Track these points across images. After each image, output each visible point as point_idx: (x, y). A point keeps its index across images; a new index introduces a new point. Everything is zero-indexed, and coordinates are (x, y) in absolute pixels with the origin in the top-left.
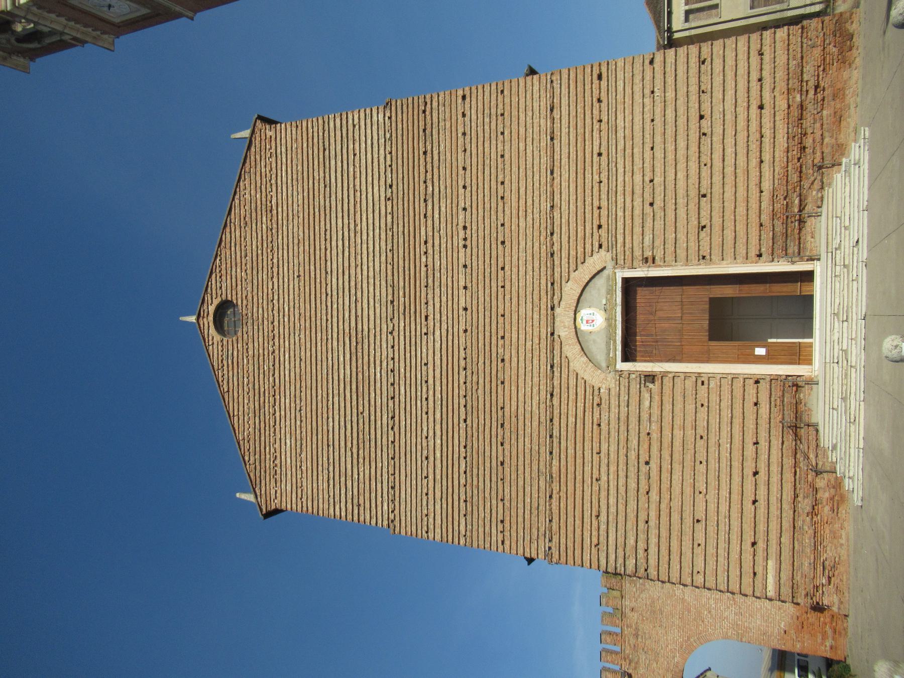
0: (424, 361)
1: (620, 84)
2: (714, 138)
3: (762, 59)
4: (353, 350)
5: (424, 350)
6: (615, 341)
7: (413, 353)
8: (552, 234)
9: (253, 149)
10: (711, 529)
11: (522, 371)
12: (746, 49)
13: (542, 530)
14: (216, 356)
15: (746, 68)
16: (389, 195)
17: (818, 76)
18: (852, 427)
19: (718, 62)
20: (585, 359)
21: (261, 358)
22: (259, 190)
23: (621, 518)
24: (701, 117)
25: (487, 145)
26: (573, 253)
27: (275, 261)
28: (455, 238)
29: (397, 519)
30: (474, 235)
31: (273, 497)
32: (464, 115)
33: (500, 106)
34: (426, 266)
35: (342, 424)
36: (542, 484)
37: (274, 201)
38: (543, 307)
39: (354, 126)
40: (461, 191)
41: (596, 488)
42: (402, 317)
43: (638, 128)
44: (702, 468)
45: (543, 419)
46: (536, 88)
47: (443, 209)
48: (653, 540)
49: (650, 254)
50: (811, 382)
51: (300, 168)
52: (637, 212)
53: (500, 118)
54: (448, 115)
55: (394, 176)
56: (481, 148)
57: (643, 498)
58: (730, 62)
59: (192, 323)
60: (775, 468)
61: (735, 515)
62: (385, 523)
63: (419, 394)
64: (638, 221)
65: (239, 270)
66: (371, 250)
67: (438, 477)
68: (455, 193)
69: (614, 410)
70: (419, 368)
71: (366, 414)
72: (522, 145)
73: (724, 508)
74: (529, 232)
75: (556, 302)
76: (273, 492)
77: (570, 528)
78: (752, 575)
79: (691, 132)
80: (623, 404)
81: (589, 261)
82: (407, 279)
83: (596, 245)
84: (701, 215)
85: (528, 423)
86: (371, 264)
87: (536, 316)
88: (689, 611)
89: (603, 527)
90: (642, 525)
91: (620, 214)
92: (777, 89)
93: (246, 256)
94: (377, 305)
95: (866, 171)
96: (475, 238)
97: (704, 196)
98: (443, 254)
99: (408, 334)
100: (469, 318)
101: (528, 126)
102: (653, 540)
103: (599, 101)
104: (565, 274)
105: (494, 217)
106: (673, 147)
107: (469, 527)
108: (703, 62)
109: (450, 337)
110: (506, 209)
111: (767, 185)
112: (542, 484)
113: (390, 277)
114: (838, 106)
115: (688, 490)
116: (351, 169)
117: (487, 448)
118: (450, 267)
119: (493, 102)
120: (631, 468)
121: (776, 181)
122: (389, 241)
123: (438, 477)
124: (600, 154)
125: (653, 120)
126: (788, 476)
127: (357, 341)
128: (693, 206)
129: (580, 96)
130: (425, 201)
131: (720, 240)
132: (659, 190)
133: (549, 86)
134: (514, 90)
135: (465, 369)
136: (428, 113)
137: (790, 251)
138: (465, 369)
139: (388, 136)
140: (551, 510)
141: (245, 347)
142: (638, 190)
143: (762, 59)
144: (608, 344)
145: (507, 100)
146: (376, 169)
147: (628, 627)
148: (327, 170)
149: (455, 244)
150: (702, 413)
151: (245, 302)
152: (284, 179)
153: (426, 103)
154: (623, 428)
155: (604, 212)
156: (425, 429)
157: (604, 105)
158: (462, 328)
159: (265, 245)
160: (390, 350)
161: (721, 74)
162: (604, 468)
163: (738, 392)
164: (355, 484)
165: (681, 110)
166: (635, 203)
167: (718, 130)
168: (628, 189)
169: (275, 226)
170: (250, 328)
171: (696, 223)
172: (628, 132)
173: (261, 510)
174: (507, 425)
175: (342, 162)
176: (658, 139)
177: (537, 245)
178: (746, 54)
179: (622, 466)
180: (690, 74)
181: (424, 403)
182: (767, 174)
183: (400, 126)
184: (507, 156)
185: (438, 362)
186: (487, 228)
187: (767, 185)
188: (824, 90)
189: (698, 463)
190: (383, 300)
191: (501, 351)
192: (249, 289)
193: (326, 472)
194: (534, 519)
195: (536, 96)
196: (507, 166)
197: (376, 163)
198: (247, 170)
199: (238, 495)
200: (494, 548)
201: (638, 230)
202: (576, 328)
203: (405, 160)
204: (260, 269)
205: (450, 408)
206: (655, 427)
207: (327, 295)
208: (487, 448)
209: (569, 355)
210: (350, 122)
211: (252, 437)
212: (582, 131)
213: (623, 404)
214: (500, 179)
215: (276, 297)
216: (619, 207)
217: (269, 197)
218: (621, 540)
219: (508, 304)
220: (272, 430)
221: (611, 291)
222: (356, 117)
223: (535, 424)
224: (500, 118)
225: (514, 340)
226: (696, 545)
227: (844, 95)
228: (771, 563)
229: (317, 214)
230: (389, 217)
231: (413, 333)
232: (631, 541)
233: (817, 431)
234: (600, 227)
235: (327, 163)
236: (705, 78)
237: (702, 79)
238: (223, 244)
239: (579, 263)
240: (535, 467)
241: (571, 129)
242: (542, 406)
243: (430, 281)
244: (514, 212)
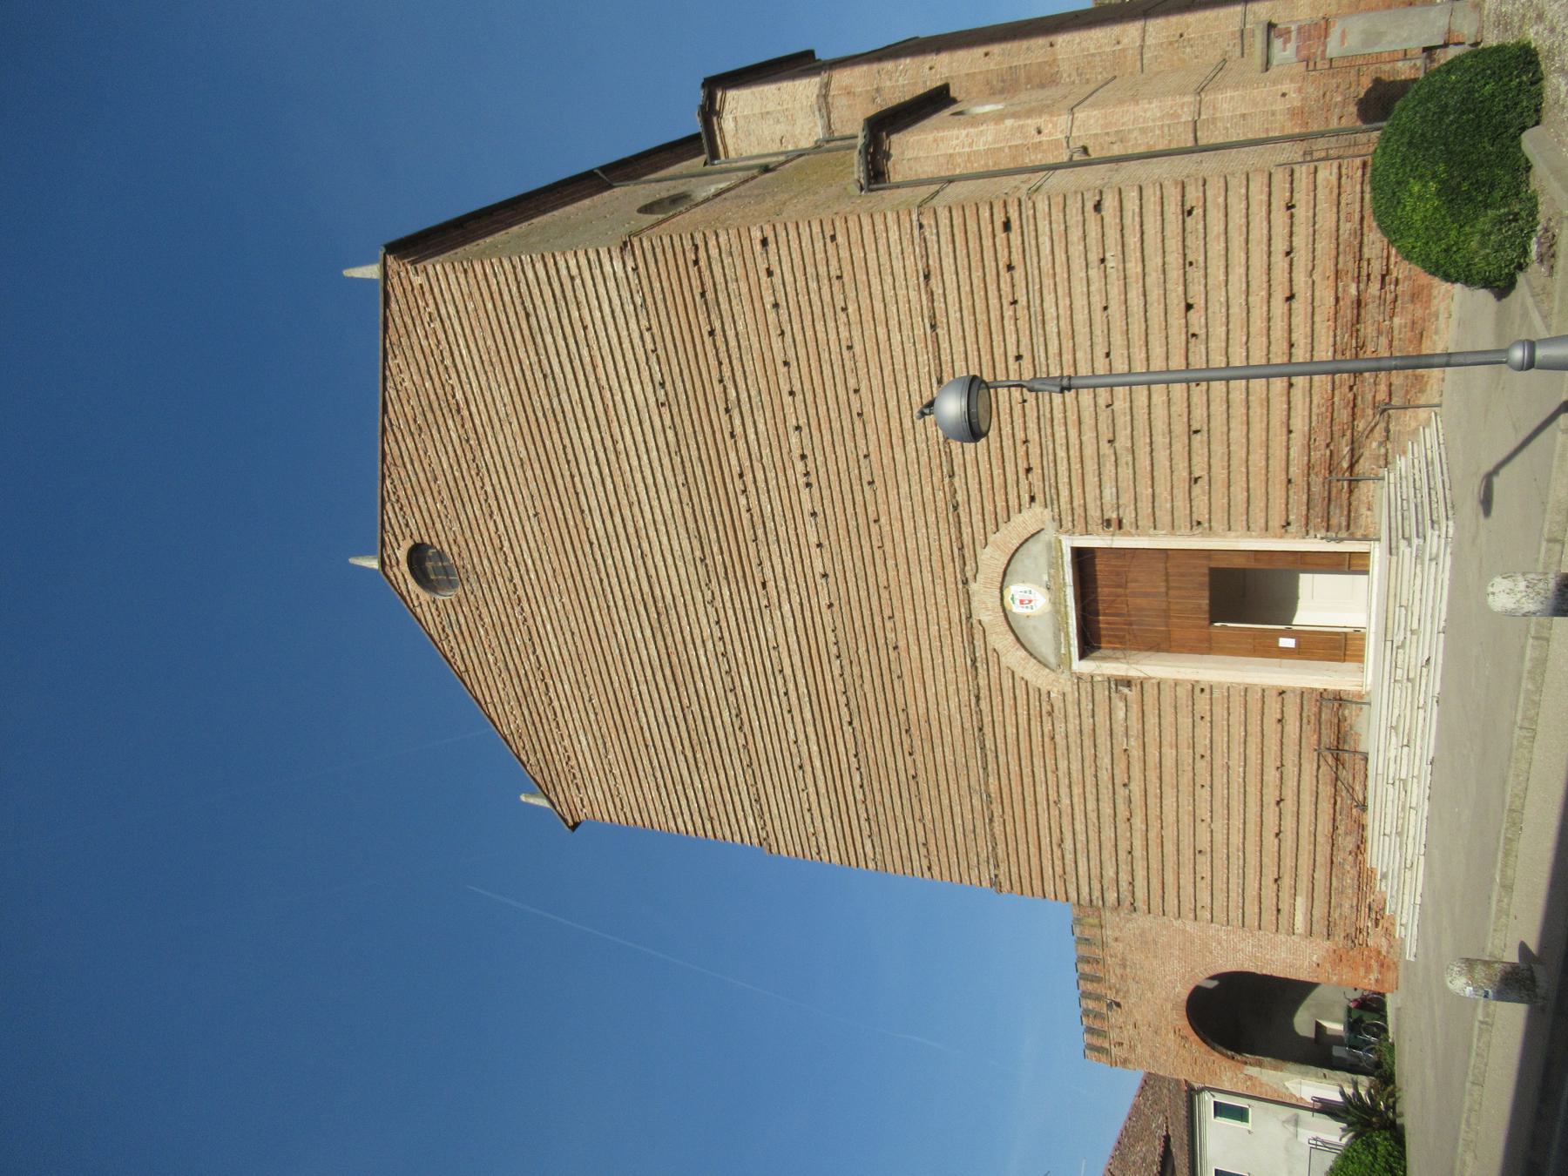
0: (772, 644)
1: (1045, 241)
2: (1212, 345)
3: (1292, 216)
4: (656, 625)
5: (769, 629)
6: (1067, 635)
7: (753, 633)
8: (952, 476)
9: (393, 305)
10: (1220, 863)
11: (927, 664)
12: (1264, 197)
13: (983, 855)
14: (429, 617)
15: (1265, 232)
16: (662, 398)
17: (1388, 258)
18: (1408, 874)
19: (1215, 216)
20: (1023, 653)
21: (507, 628)
22: (426, 377)
23: (1094, 846)
24: (1189, 307)
25: (819, 326)
26: (989, 507)
27: (489, 489)
28: (790, 472)
29: (772, 837)
30: (822, 471)
31: (579, 806)
32: (770, 273)
33: (834, 263)
34: (749, 510)
35: (661, 720)
36: (976, 802)
37: (459, 396)
38: (950, 579)
39: (572, 279)
40: (788, 399)
41: (1054, 812)
42: (724, 583)
43: (1081, 317)
44: (1206, 793)
45: (967, 725)
46: (894, 236)
47: (761, 427)
49: (1114, 516)
50: (1360, 701)
51: (490, 342)
52: (1089, 451)
53: (836, 283)
54: (740, 271)
55: (665, 369)
56: (809, 333)
57: (1122, 826)
58: (1237, 218)
59: (372, 570)
60: (1307, 798)
61: (1252, 847)
62: (755, 841)
63: (773, 687)
64: (1091, 466)
65: (430, 500)
66: (650, 481)
67: (822, 790)
68: (777, 401)
70: (766, 654)
71: (695, 707)
72: (881, 331)
73: (1236, 839)
74: (913, 469)
75: (969, 574)
76: (577, 800)
77: (1023, 857)
79: (1173, 332)
80: (1086, 714)
81: (1017, 519)
82: (721, 528)
83: (1026, 498)
84: (1194, 462)
85: (946, 730)
86: (655, 503)
87: (940, 592)
88: (1192, 943)
89: (1069, 857)
90: (1123, 855)
91: (1061, 454)
92: (1318, 270)
93: (436, 479)
94: (680, 564)
95: (1447, 582)
96: (822, 471)
97: (1196, 432)
98: (775, 494)
99: (738, 606)
100: (833, 589)
101: (888, 299)
103: (1010, 268)
104: (979, 537)
105: (850, 445)
106: (1143, 355)
107: (878, 850)
108: (1190, 213)
109: (807, 614)
110: (869, 432)
111: (1299, 424)
112: (976, 802)
113: (691, 525)
114: (1419, 313)
115: (1186, 819)
116: (585, 352)
117: (890, 759)
118: (789, 515)
119: (820, 256)
120: (1103, 790)
121: (1314, 418)
122: (679, 470)
123: (822, 790)
124: (1019, 358)
125: (1106, 308)
126: (1325, 806)
127: (660, 616)
128: (1179, 447)
129: (975, 258)
130: (727, 410)
131: (1225, 500)
132: (1123, 421)
133: (916, 232)
134: (855, 236)
135: (838, 657)
136: (703, 263)
137: (1334, 521)
138: (838, 657)
139: (639, 301)
140: (993, 835)
141: (476, 613)
143: (1292, 216)
144: (1056, 637)
145: (844, 254)
146: (629, 356)
148: (542, 351)
149: (792, 482)
150: (1203, 729)
151: (455, 549)
152: (467, 360)
153: (696, 248)
154: (1088, 743)
155: (1034, 450)
156: (791, 732)
157: (1019, 273)
158: (824, 602)
159: (464, 466)
160: (715, 629)
161: (1222, 238)
162: (1064, 791)
163: (1254, 707)
164: (700, 795)
165: (1155, 294)
166: (1084, 438)
167: (1218, 331)
168: (1072, 417)
169: (472, 435)
170: (476, 586)
171: (1185, 474)
172: (1065, 324)
173: (565, 821)
174: (914, 730)
175: (565, 338)
176: (1118, 339)
177: (928, 490)
178: (1264, 208)
179: (1090, 788)
180: (1168, 233)
181: (784, 699)
182: (1300, 406)
183: (656, 285)
184: (858, 348)
185: (794, 647)
186: (841, 460)
187: (1299, 424)
188: (1397, 282)
189: (1198, 787)
190: (689, 557)
191: (890, 635)
192: (456, 528)
193: (651, 778)
194: (971, 844)
195: (896, 250)
196: (861, 364)
197: (626, 345)
198: (394, 338)
199: (523, 798)
200: (917, 873)
201: (1092, 479)
202: (1004, 610)
203: (679, 343)
204: (466, 499)
205: (824, 706)
207: (591, 544)
208: (890, 759)
209: (998, 647)
210: (564, 272)
211: (524, 731)
212: (985, 318)
213: (1086, 714)
214: (852, 383)
215: (506, 544)
216: (1058, 442)
217: (448, 388)
218: (1095, 872)
219: (892, 573)
220: (553, 725)
221: (1055, 564)
222: (572, 263)
223: (957, 731)
224: (836, 283)
225: (910, 622)
227: (1429, 295)
228: (1301, 901)
229: (542, 420)
230: (670, 434)
231: (747, 606)
232: (1110, 872)
233: (1366, 759)
234: (1029, 470)
235: (539, 340)
236: (1195, 243)
237: (1188, 243)
238: (389, 458)
240: (964, 784)
241: (965, 313)
242: (965, 710)
243: (760, 532)
244: (883, 437)
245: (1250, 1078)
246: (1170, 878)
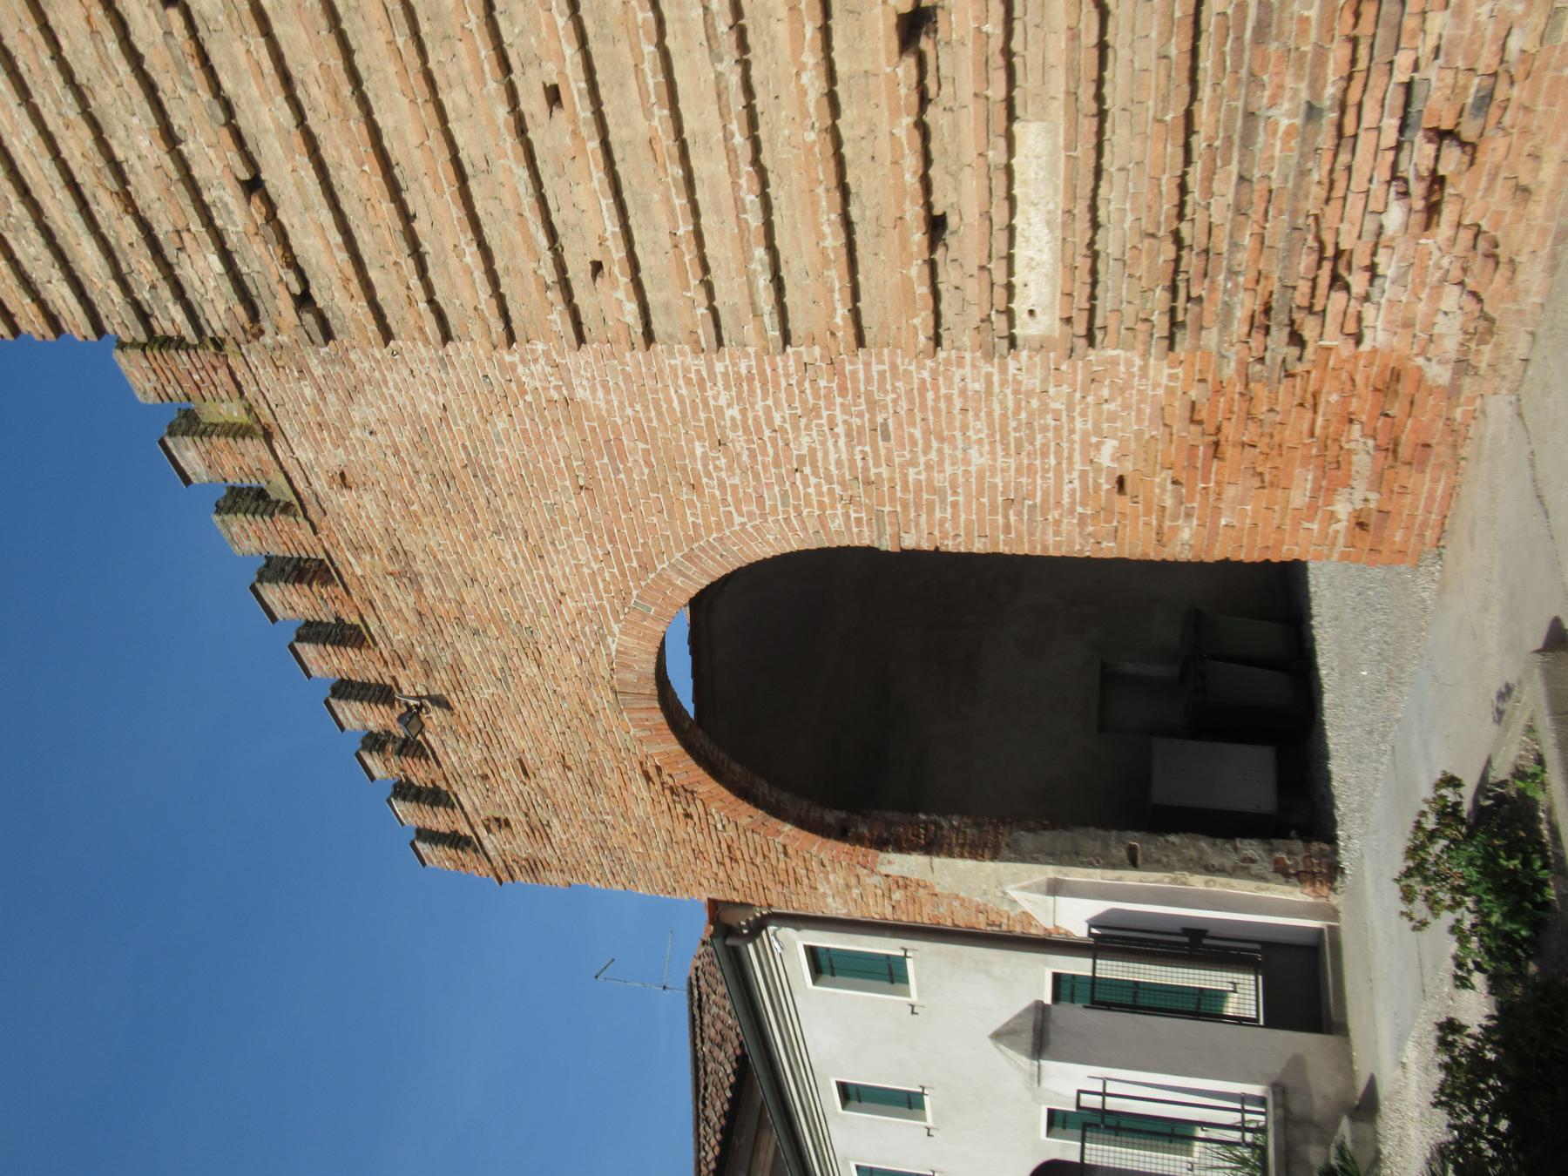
48: (265, 117)
78: (918, 238)
88: (618, 455)
102: (265, 117)
147: (356, 549)
226: (532, 103)
228: (1040, 146)
245: (903, 883)
246: (401, 117)
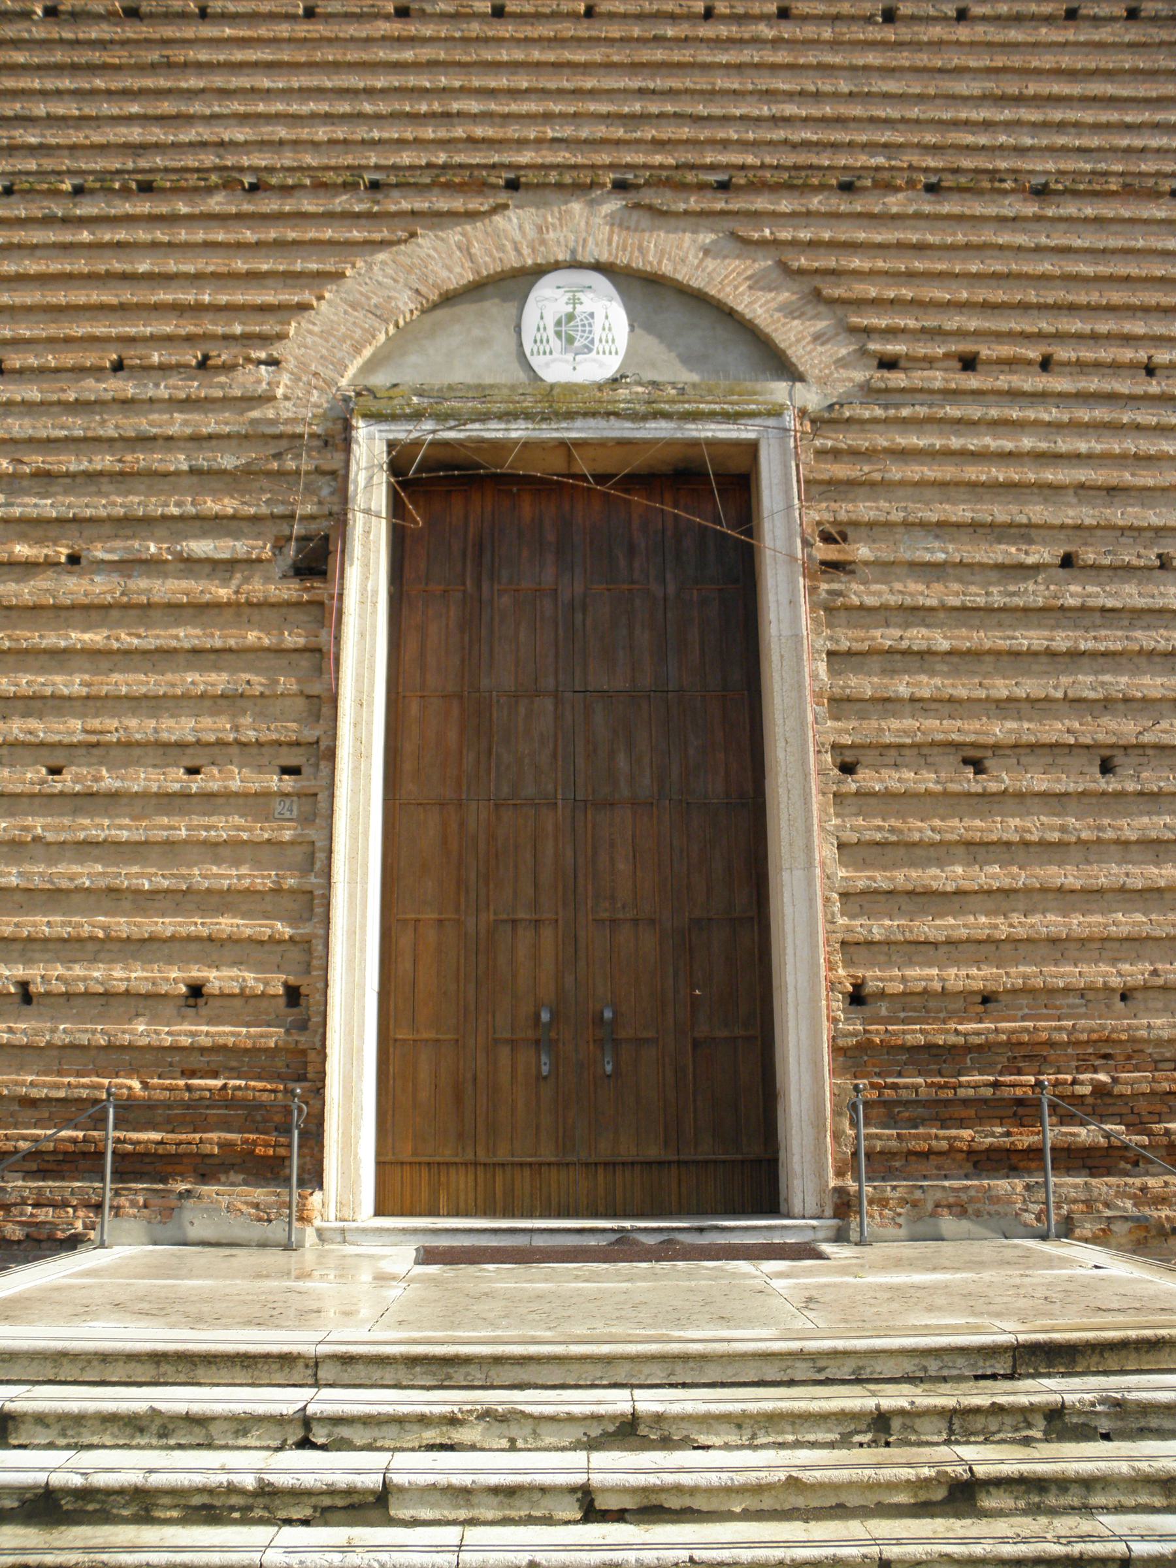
52: (1038, 512)
69: (178, 424)
75: (649, 197)
132: (1131, 594)
142: (1120, 514)
206: (99, 587)
223: (135, 134)
239: (818, 282)
